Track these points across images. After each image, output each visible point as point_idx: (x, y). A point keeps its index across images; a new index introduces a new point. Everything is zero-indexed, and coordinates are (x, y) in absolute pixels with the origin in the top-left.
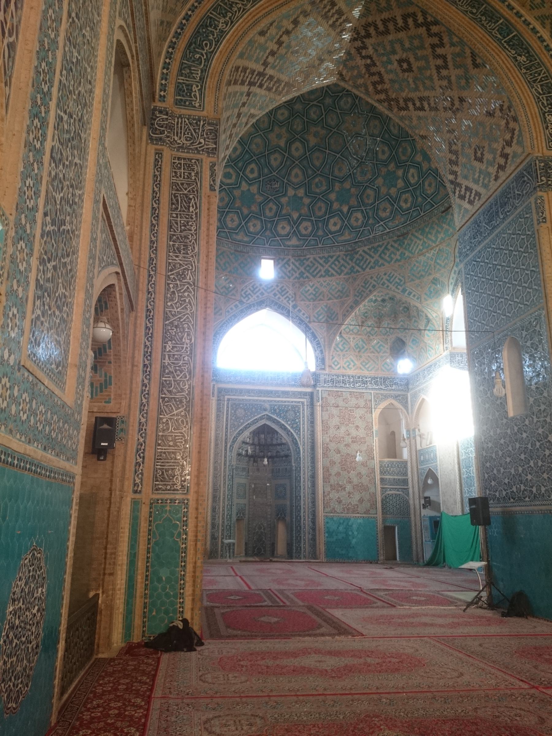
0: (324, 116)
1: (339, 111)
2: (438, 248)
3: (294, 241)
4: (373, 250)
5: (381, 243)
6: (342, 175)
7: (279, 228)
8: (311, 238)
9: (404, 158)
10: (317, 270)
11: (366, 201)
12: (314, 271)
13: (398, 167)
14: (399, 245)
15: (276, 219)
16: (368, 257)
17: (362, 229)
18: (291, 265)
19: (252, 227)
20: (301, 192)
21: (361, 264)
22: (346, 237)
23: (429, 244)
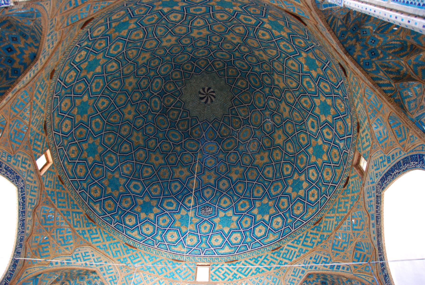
0: (240, 159)
1: (250, 153)
2: (350, 216)
3: (227, 250)
4: (296, 242)
5: (301, 235)
6: (260, 195)
7: (213, 241)
8: (241, 245)
9: (302, 166)
10: (249, 270)
11: (282, 207)
12: (245, 272)
13: (300, 174)
14: (317, 230)
15: (210, 234)
16: (292, 249)
17: (283, 229)
18: (225, 269)
19: (189, 241)
20: (230, 213)
21: (288, 256)
22: (272, 237)
23: (342, 217)
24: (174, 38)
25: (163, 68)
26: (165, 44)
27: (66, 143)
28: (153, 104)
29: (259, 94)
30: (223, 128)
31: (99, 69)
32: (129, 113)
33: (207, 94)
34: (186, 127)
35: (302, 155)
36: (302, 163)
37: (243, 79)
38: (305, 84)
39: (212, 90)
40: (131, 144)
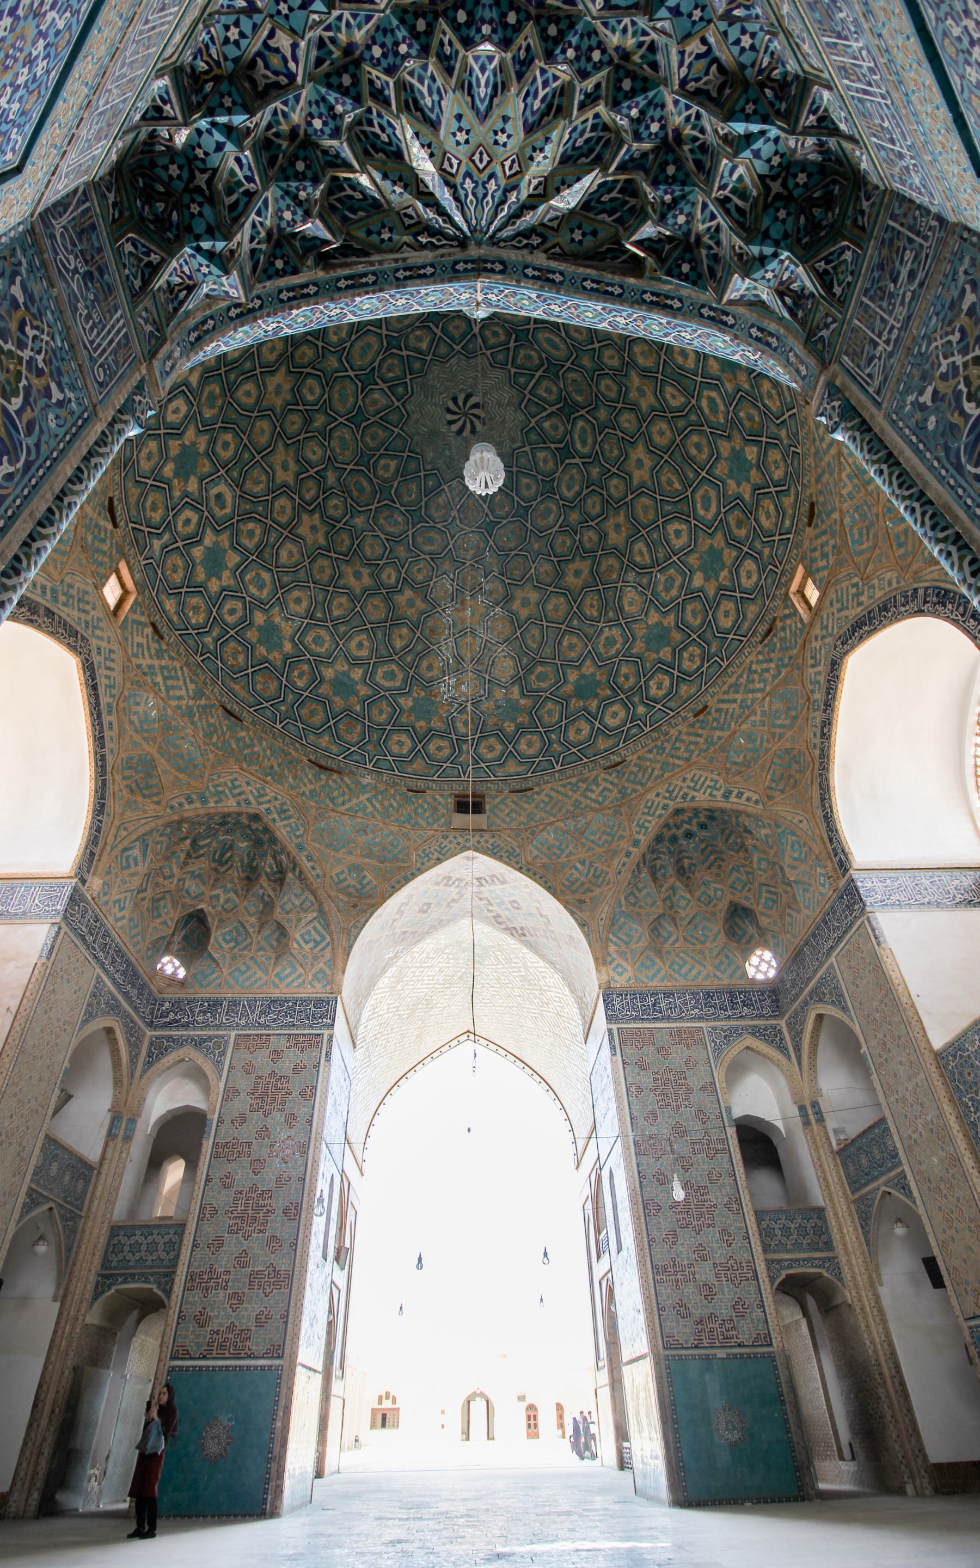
24: (516, 605)
25: (552, 518)
26: (534, 596)
27: (767, 551)
28: (590, 441)
29: (346, 460)
30: (424, 346)
31: (654, 617)
32: (640, 463)
33: (466, 414)
34: (522, 352)
35: (215, 411)
36: (211, 394)
37: (386, 480)
38: (266, 576)
39: (455, 428)
40: (659, 393)
